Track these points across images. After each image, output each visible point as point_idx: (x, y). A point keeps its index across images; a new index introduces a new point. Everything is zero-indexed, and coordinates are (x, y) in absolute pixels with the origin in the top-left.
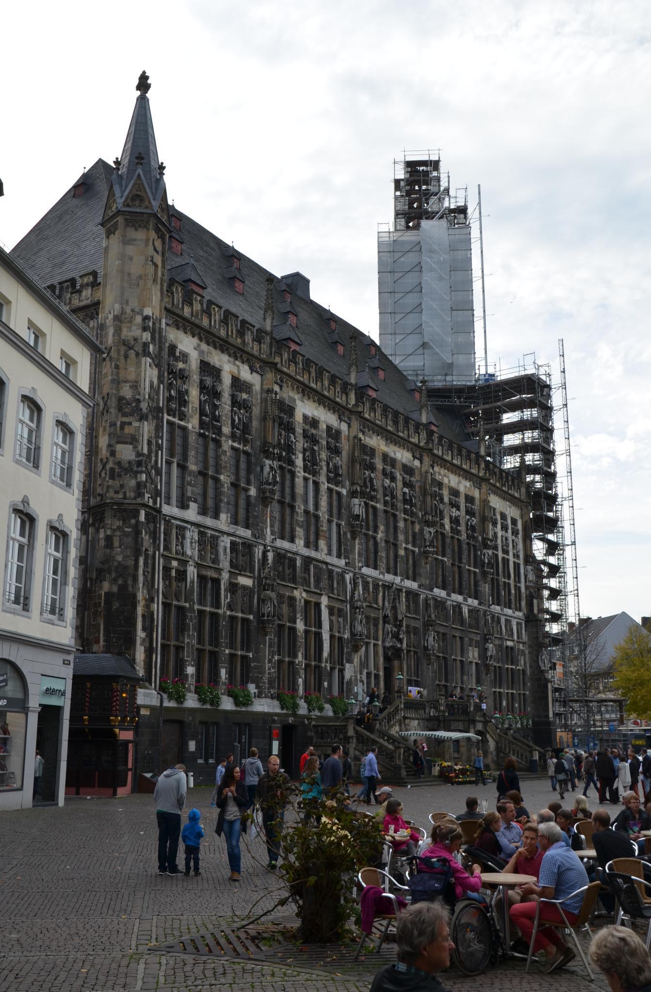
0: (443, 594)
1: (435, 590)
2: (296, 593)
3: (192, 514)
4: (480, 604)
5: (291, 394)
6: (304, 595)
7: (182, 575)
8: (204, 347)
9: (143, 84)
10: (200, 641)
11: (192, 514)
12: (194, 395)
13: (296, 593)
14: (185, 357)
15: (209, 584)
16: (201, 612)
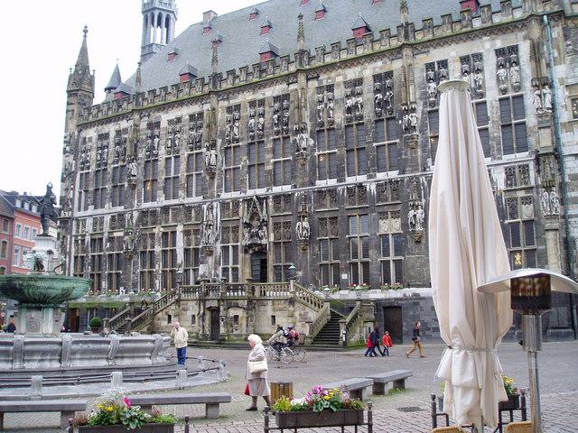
0: (332, 182)
1: (318, 182)
2: (156, 231)
3: (91, 210)
4: (403, 172)
5: (157, 114)
6: (162, 229)
7: (83, 241)
8: (100, 127)
9: (85, 31)
10: (93, 270)
11: (91, 210)
12: (93, 155)
13: (156, 231)
14: (90, 139)
15: (96, 242)
16: (93, 256)
